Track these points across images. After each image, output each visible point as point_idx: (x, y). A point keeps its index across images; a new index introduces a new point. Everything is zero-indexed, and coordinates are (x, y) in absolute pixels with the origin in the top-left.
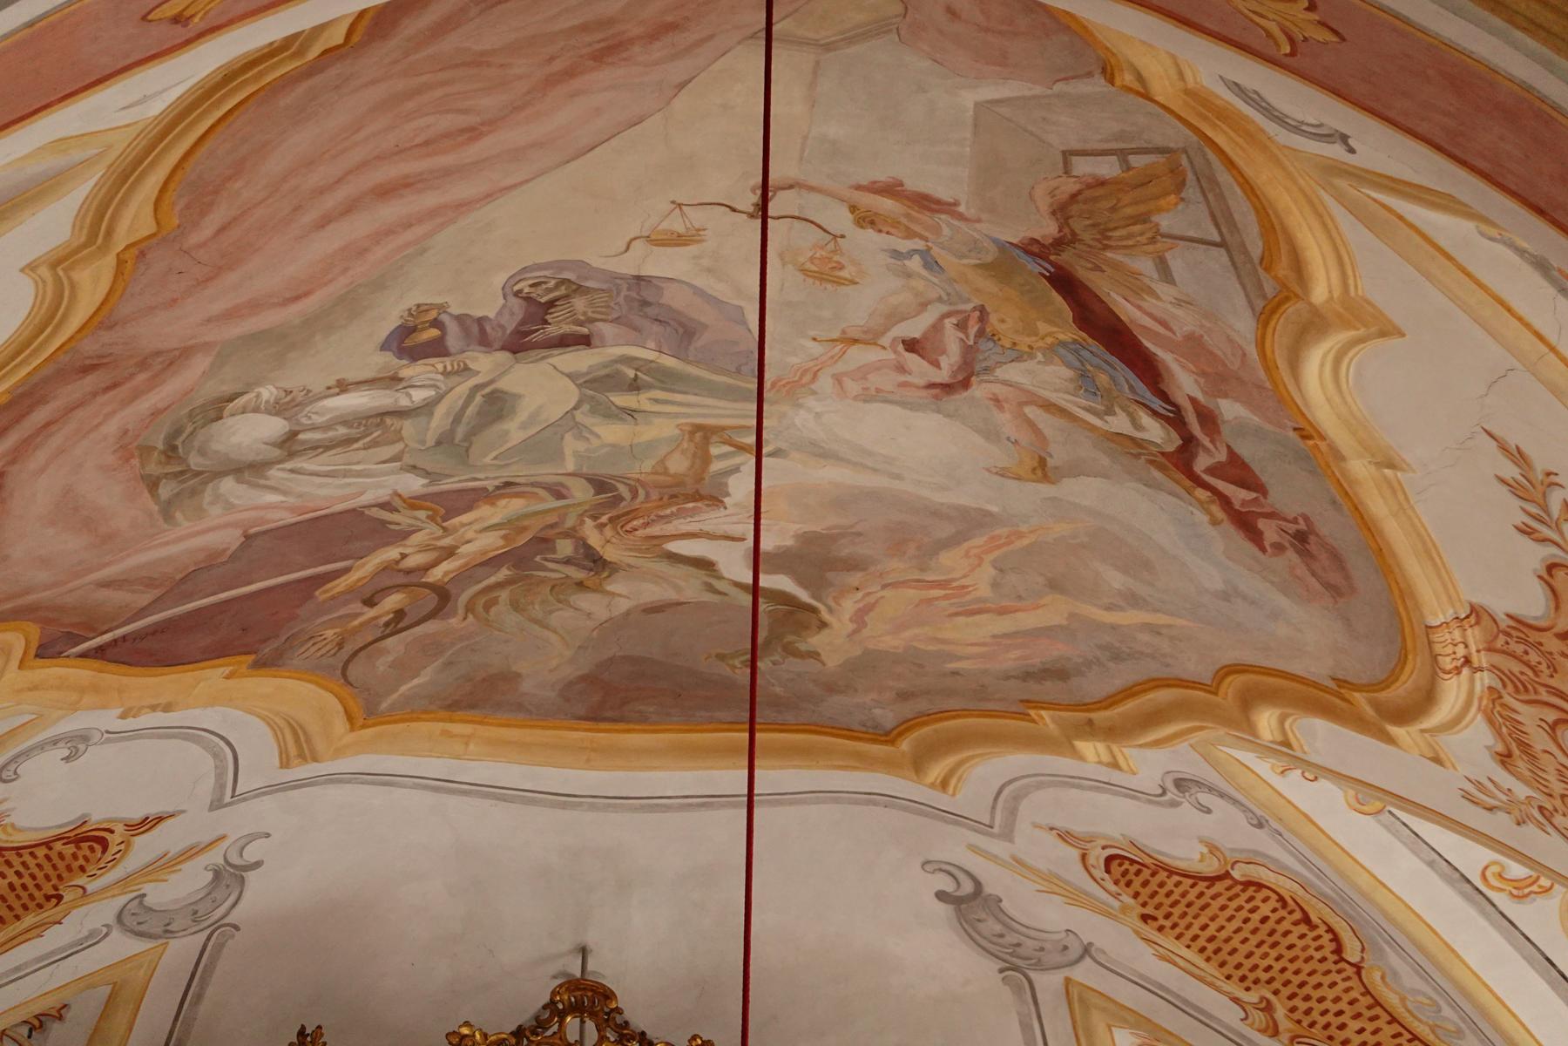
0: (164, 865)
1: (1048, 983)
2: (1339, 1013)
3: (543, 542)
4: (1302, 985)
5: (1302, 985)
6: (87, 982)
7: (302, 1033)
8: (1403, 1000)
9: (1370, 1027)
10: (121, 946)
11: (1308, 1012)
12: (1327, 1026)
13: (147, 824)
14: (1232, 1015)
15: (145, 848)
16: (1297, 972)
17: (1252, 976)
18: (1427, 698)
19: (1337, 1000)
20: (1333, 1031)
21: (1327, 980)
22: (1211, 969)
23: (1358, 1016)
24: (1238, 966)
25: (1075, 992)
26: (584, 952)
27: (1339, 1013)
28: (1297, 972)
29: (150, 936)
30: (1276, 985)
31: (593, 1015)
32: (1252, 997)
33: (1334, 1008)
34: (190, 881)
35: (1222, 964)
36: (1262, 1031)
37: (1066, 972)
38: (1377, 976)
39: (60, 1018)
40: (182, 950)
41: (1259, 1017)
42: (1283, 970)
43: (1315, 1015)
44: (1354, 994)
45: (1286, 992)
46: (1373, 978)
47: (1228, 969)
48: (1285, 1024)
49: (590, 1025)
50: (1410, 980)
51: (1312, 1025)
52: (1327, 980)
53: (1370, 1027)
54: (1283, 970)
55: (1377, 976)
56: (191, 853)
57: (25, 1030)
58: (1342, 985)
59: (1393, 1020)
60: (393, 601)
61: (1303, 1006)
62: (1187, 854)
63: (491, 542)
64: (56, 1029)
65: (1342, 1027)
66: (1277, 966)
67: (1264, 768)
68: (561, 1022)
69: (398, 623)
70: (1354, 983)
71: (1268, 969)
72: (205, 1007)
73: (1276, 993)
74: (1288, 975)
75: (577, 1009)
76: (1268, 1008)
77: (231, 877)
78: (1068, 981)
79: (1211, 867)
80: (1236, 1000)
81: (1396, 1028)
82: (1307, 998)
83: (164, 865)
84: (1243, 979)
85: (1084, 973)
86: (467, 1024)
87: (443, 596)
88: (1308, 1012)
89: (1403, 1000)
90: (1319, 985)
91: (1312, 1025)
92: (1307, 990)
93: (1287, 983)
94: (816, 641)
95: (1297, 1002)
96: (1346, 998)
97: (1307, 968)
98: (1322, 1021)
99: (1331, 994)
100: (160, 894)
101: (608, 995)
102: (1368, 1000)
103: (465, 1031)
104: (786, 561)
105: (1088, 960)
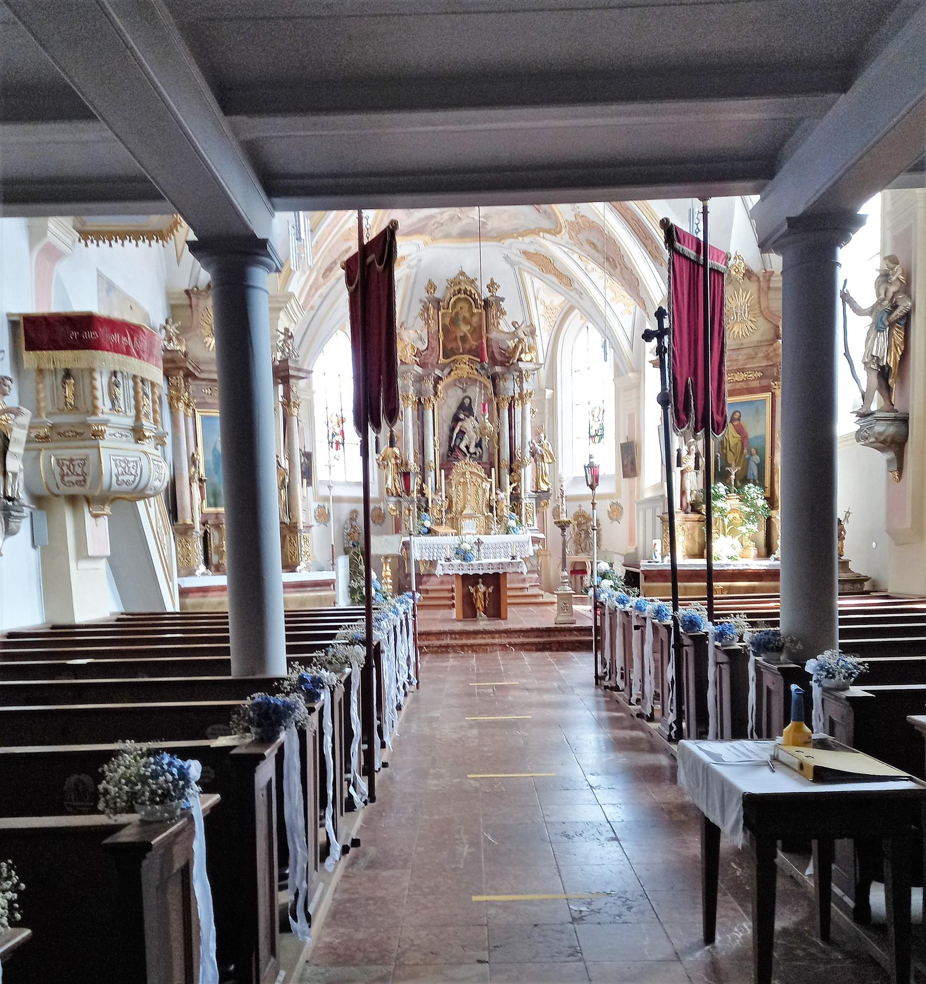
0: (412, 260)
1: (516, 268)
3: (454, 217)
10: (408, 270)
13: (409, 255)
15: (409, 258)
18: (560, 231)
34: (415, 262)
40: (415, 270)
56: (415, 258)
60: (436, 226)
62: (532, 251)
63: (448, 217)
67: (541, 240)
69: (437, 228)
77: (420, 261)
79: (535, 252)
83: (412, 260)
85: (521, 266)
87: (442, 224)
94: (487, 226)
100: (411, 264)
104: (482, 217)
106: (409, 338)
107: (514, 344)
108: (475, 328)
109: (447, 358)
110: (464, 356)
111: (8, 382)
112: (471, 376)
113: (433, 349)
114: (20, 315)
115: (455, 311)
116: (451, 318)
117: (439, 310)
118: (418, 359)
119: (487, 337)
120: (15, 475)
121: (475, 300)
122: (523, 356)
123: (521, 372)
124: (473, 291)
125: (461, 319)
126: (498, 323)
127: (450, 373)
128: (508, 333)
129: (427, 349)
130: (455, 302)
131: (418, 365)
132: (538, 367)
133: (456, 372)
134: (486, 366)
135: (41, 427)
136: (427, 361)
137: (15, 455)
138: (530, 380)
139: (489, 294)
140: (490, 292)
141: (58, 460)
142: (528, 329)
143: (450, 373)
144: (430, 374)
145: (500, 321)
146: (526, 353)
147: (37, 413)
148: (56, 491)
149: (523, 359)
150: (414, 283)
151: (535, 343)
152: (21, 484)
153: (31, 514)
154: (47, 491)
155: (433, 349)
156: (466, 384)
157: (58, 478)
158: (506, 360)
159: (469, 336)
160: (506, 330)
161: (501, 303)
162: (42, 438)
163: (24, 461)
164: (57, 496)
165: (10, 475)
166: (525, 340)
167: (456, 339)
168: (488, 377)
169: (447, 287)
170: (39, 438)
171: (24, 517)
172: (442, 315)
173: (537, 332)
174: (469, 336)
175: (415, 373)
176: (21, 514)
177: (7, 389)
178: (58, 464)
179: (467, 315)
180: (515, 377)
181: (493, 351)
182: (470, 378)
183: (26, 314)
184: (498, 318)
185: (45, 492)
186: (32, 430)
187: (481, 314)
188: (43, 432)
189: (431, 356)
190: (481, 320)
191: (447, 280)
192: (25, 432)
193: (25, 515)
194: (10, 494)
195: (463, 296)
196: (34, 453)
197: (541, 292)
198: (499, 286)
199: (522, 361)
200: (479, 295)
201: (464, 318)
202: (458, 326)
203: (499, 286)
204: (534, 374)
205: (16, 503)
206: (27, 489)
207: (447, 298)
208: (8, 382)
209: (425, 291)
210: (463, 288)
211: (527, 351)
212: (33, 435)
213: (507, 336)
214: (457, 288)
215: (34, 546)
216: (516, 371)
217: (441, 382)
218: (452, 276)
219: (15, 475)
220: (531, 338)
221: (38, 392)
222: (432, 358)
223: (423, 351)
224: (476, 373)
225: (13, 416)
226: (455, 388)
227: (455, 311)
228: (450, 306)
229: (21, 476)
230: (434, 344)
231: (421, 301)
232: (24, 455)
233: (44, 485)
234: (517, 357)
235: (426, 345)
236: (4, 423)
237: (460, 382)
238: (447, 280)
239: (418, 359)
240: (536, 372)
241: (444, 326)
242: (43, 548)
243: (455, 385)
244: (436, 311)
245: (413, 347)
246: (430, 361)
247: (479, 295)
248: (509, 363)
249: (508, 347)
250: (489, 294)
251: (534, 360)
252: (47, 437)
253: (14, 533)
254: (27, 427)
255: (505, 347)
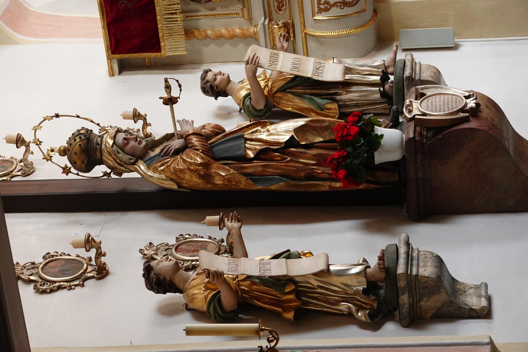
111: (210, 76)
114: (109, 59)
120: (348, 70)
135: (272, 33)
137: (317, 70)
141: (320, 11)
147: (253, 39)
148: (369, 13)
152: (362, 62)
153: (405, 50)
154: (365, 29)
157: (348, 10)
162: (288, 32)
163: (325, 58)
164: (375, 11)
165: (348, 77)
170: (289, 35)
171: (413, 59)
176: (408, 64)
177: (219, 78)
178: (326, 10)
183: (107, 51)
185: (370, 31)
186: (278, 45)
188: (278, 32)
192: (281, 53)
193: (409, 57)
194: (378, 78)
196: (312, 44)
205: (390, 70)
206: (366, 54)
208: (210, 76)
212: (285, 45)
215: (455, 48)
219: (348, 70)
221: (220, 37)
225: (260, 71)
229: (349, 62)
232: (316, 57)
233: (360, 30)
236: (270, 84)
242: (456, 34)
252: (286, 25)
253: (438, 73)
254: (275, 51)
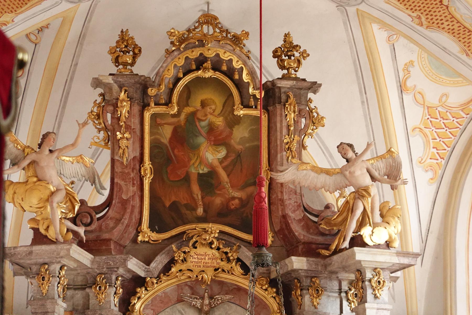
2: (442, 20)
4: (430, 11)
5: (430, 11)
6: (56, 17)
7: (122, 31)
8: (461, 16)
9: (451, 24)
11: (432, 19)
12: (438, 23)
14: (409, 20)
16: (428, 8)
17: (414, 9)
19: (441, 16)
20: (439, 25)
21: (438, 10)
22: (402, 6)
23: (447, 21)
24: (410, 5)
25: (360, 13)
26: (208, 3)
27: (442, 20)
28: (428, 8)
29: (75, 3)
30: (422, 11)
31: (211, 24)
32: (415, 14)
33: (440, 18)
35: (405, 5)
36: (418, 24)
37: (357, 7)
38: (453, 9)
39: (47, 28)
41: (417, 20)
42: (424, 7)
43: (434, 20)
44: (446, 14)
45: (425, 13)
46: (452, 10)
47: (407, 6)
48: (425, 22)
49: (211, 28)
50: (463, 11)
51: (433, 23)
52: (438, 10)
53: (451, 24)
54: (424, 7)
55: (453, 9)
57: (37, 32)
58: (442, 12)
59: (458, 22)
61: (430, 17)
64: (46, 30)
65: (442, 24)
66: (422, 6)
68: (202, 27)
70: (446, 11)
71: (419, 6)
72: (92, 23)
73: (422, 13)
74: (426, 8)
75: (207, 23)
76: (419, 18)
78: (357, 9)
80: (409, 15)
81: (459, 25)
82: (432, 15)
84: (412, 9)
86: (173, 29)
88: (432, 19)
89: (461, 16)
90: (435, 12)
91: (433, 23)
92: (431, 13)
93: (425, 11)
95: (428, 16)
96: (444, 15)
97: (431, 6)
98: (436, 22)
99: (439, 14)
101: (216, 18)
102: (450, 16)
103: (172, 31)
105: (363, 3)
106: (60, 174)
107: (341, 202)
108: (239, 156)
109: (159, 232)
110: (210, 226)
112: (224, 277)
113: (124, 203)
115: (188, 110)
116: (175, 131)
117: (145, 106)
118: (81, 230)
119: (271, 181)
121: (240, 85)
122: (366, 232)
123: (360, 272)
124: (237, 65)
125: (204, 132)
126: (302, 146)
127: (166, 269)
128: (327, 172)
129: (108, 203)
130: (187, 87)
131: (81, 244)
132: (405, 261)
133: (184, 267)
134: (269, 256)
136: (106, 236)
138: (384, 294)
139: (279, 73)
140: (282, 67)
142: (381, 165)
143: (166, 269)
144: (111, 270)
145: (308, 141)
146: (375, 225)
149: (367, 240)
150: (82, 37)
151: (399, 200)
155: (124, 203)
156: (211, 298)
158: (320, 239)
159: (223, 174)
160: (324, 164)
161: (310, 95)
166: (373, 191)
167: (187, 179)
168: (273, 283)
169: (168, 52)
172: (154, 117)
173: (405, 173)
174: (223, 174)
175: (72, 265)
179: (219, 122)
180: (345, 286)
181: (285, 217)
182: (222, 283)
184: (303, 132)
187: (258, 120)
189: (118, 221)
190: (256, 135)
191: (171, 34)
195: (209, 74)
197: (415, 71)
198: (305, 55)
199: (364, 245)
200: (252, 73)
201: (211, 129)
202: (195, 148)
203: (305, 55)
204: (395, 279)
207: (170, 75)
209: (110, 57)
210: (210, 54)
211: (378, 219)
213: (323, 178)
214: (194, 54)
216: (345, 269)
217: (141, 291)
218: (182, 28)
220: (387, 187)
222: (120, 227)
223: (98, 209)
224: (238, 270)
226: (179, 306)
227: (188, 110)
228: (175, 98)
230: (133, 189)
231: (97, 83)
234: (350, 234)
235: (106, 193)
237: (194, 292)
238: (171, 34)
239: (81, 230)
240: (399, 274)
241: (155, 146)
243: (180, 300)
244: (136, 109)
245: (70, 198)
246: (116, 234)
247: (252, 73)
248: (327, 247)
249: (327, 207)
250: (279, 73)
251: (396, 244)
255: (317, 207)
